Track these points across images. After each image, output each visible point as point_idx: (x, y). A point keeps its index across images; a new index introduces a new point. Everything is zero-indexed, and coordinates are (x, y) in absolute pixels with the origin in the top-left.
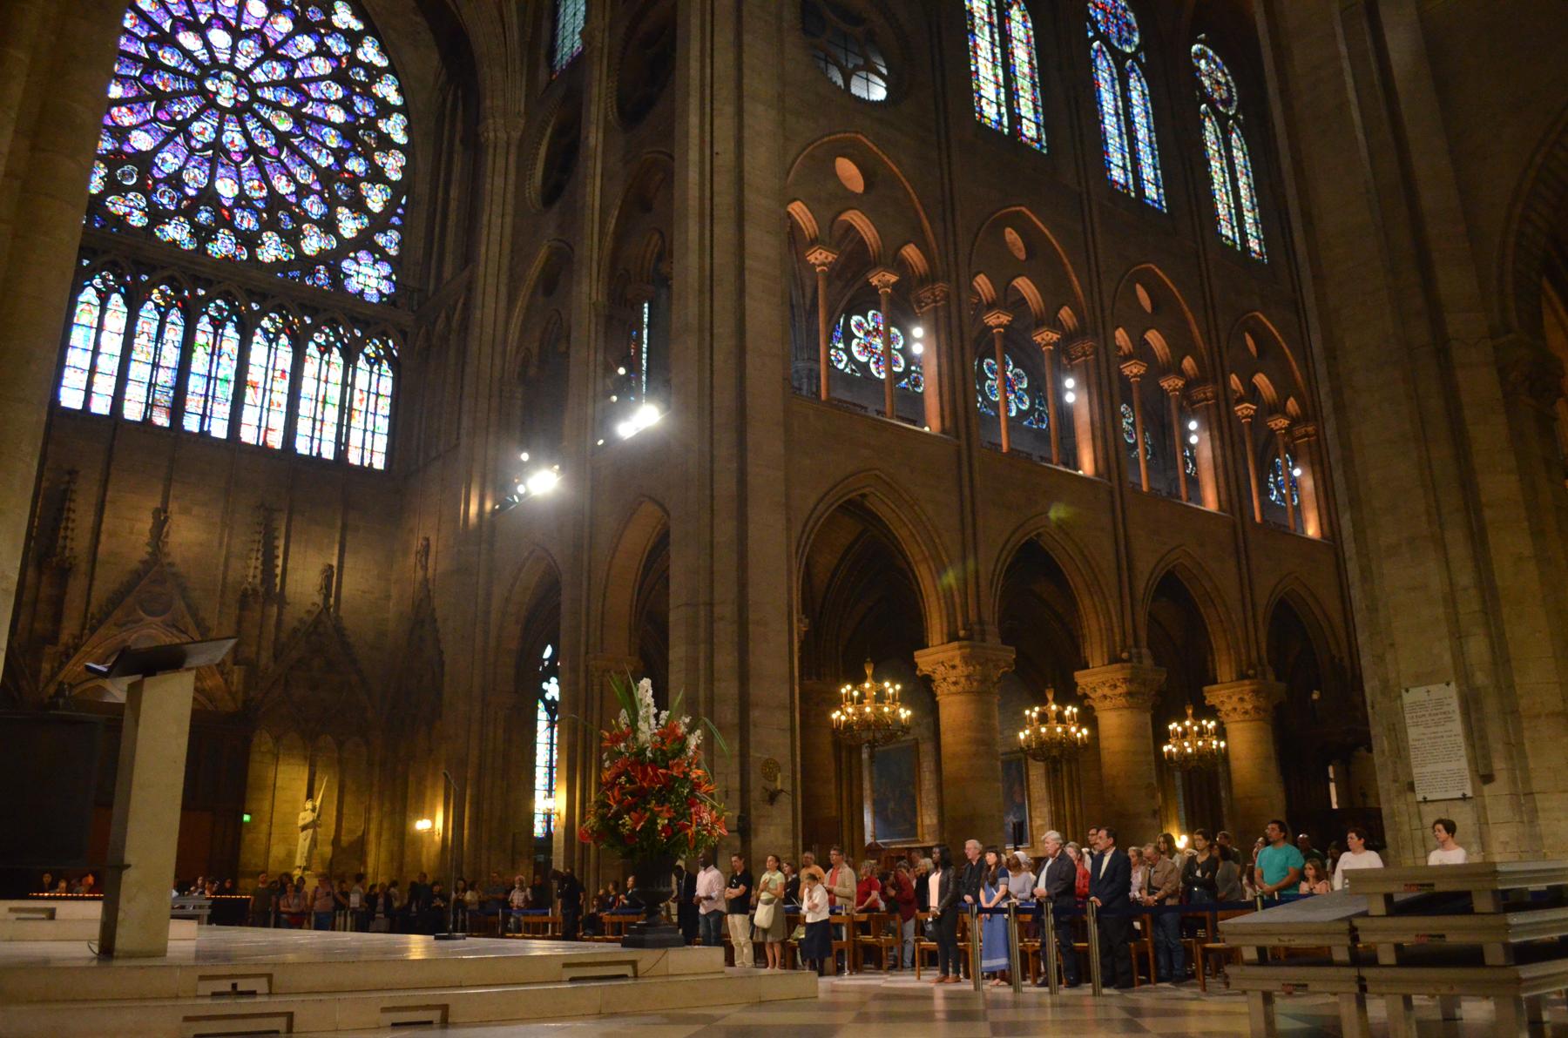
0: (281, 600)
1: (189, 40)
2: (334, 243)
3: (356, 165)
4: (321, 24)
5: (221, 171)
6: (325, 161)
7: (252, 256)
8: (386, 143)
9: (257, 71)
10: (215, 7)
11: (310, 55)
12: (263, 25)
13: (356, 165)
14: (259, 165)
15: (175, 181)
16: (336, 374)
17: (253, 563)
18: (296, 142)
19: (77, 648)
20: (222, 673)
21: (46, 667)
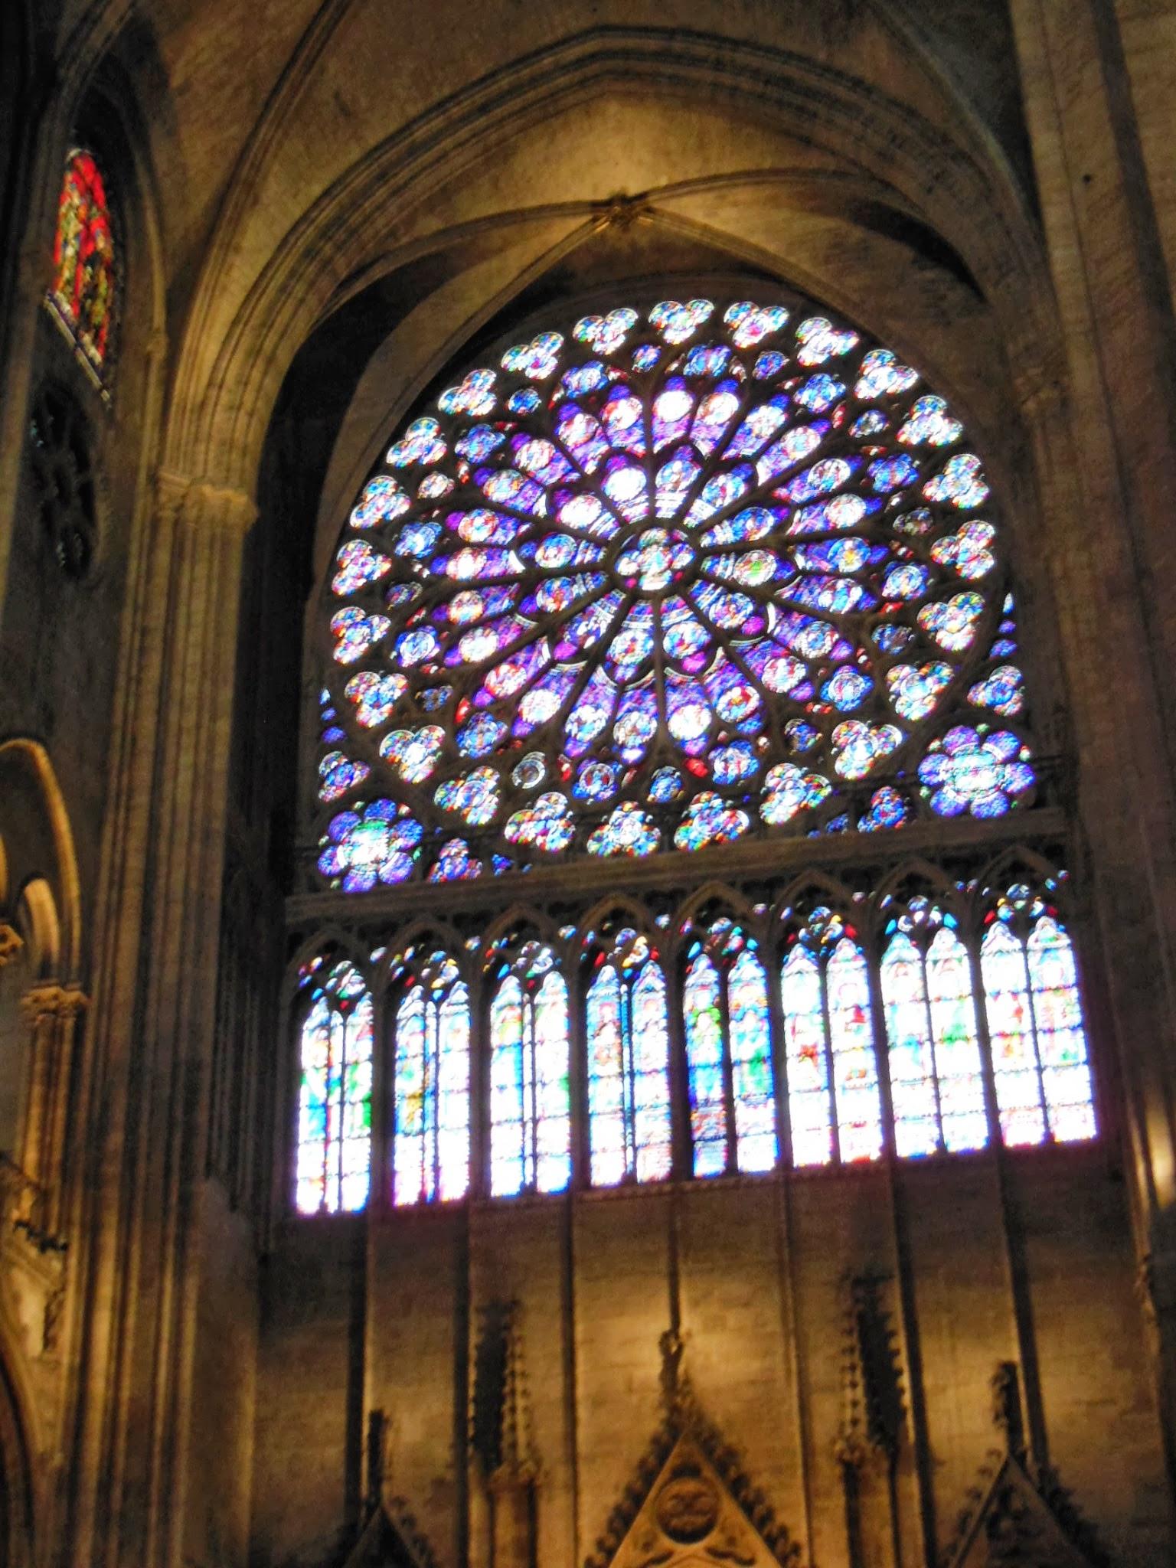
0: (926, 1461)
1: (578, 512)
2: (897, 736)
3: (903, 583)
4: (785, 373)
5: (674, 698)
6: (844, 599)
8: (949, 519)
10: (608, 439)
11: (778, 436)
12: (689, 427)
13: (903, 583)
14: (734, 660)
15: (605, 748)
17: (849, 1394)
18: (787, 593)
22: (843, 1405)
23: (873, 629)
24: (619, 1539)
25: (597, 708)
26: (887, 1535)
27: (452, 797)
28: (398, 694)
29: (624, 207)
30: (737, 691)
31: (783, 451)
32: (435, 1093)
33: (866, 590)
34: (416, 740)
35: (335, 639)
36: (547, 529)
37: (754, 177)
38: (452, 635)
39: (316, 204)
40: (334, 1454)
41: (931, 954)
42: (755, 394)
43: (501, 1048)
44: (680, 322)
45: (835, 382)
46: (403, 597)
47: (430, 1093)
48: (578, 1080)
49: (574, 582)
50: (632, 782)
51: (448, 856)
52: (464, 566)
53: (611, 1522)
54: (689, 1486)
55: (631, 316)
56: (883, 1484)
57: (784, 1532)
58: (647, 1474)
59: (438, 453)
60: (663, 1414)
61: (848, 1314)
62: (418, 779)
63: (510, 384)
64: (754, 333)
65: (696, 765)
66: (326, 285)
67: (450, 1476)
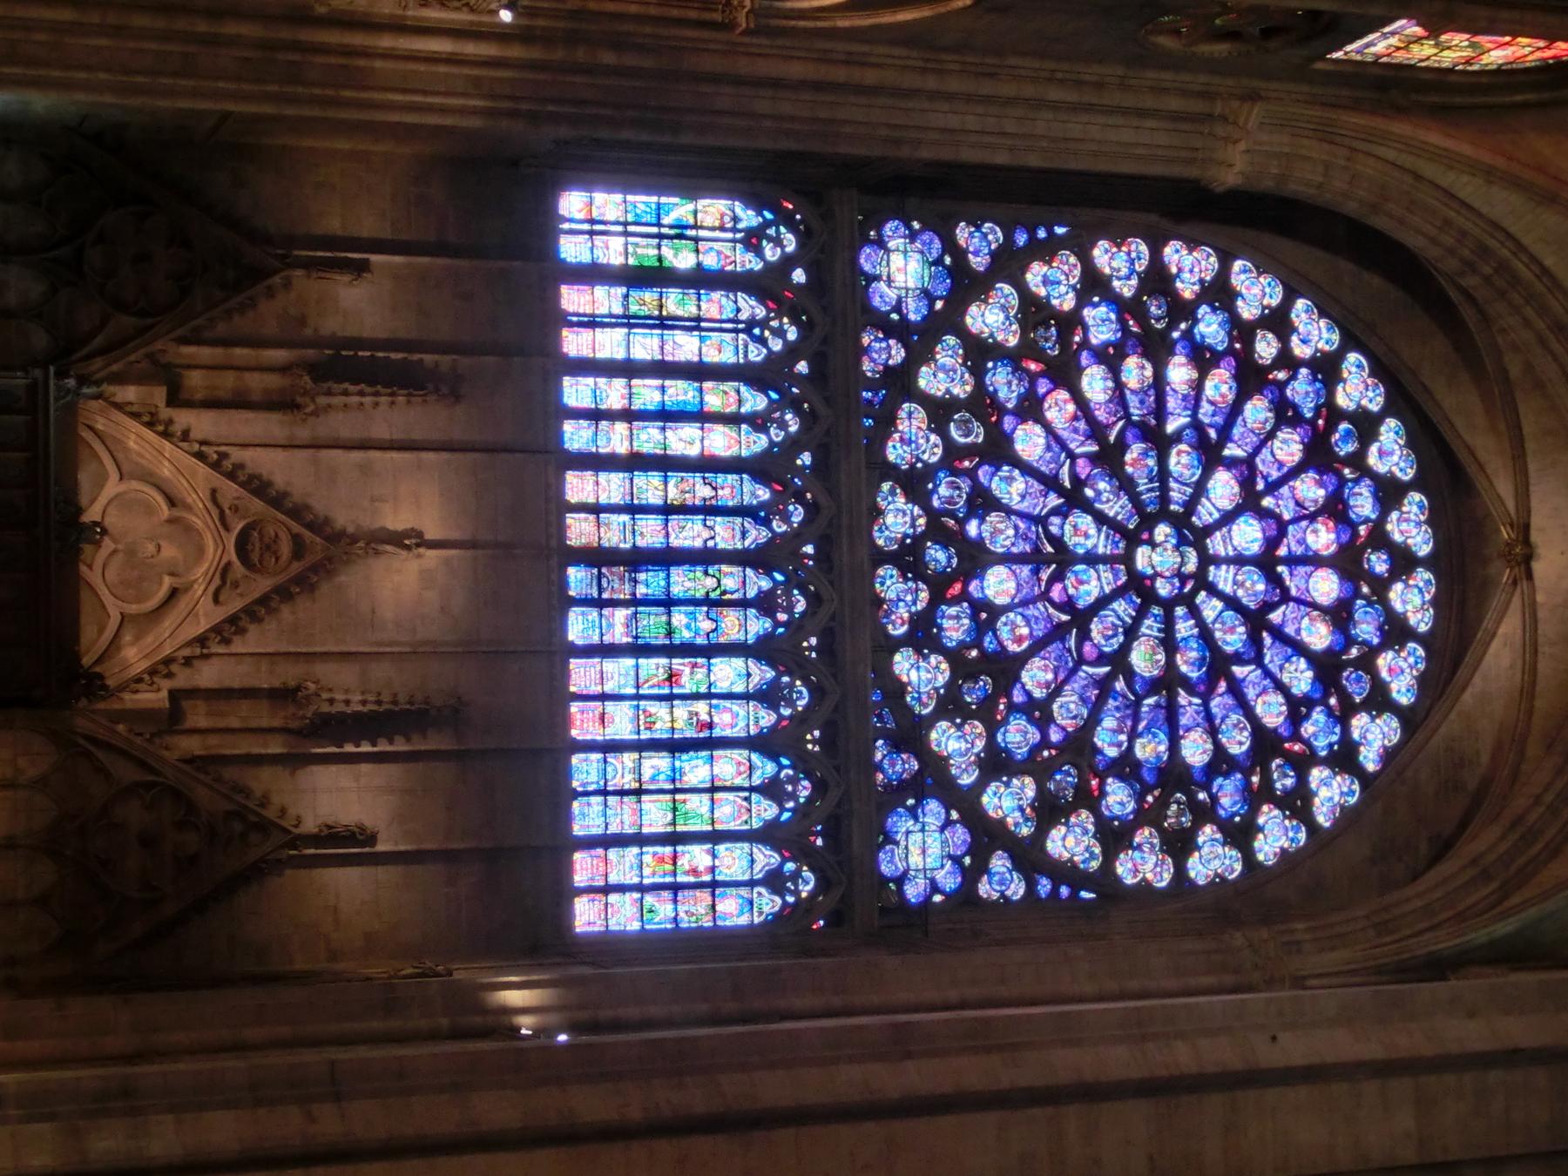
0: (296, 761)
1: (1223, 488)
2: (966, 780)
3: (1118, 798)
5: (1025, 571)
6: (1108, 741)
7: (895, 644)
8: (1179, 846)
9: (1219, 605)
10: (1296, 520)
12: (1299, 601)
13: (1118, 798)
14: (1057, 633)
15: (982, 502)
16: (729, 813)
18: (1120, 685)
19: (166, 435)
20: (153, 672)
21: (130, 393)
22: (347, 691)
23: (1074, 765)
24: (241, 485)
25: (1023, 497)
26: (235, 723)
27: (948, 352)
28: (1055, 302)
29: (1523, 558)
30: (1025, 631)
31: (1264, 692)
32: (663, 326)
33: (1114, 761)
34: (1007, 318)
35: (1118, 240)
36: (1210, 455)
37: (1528, 689)
38: (1111, 358)
39: (1534, 259)
40: (334, 224)
41: (755, 797)
42: (1327, 667)
43: (701, 390)
44: (1412, 600)
45: (1331, 745)
46: (1153, 309)
47: (663, 323)
48: (665, 464)
49: (1151, 481)
50: (944, 526)
51: (889, 346)
52: (1179, 373)
53: (258, 477)
54: (285, 549)
55: (1424, 549)
56: (276, 723)
57: (242, 631)
58: (297, 512)
59: (1300, 350)
60: (351, 529)
61: (427, 701)
62: (969, 320)
63: (1366, 425)
64: (1390, 670)
65: (958, 587)
66: (1451, 265)
67: (308, 332)
